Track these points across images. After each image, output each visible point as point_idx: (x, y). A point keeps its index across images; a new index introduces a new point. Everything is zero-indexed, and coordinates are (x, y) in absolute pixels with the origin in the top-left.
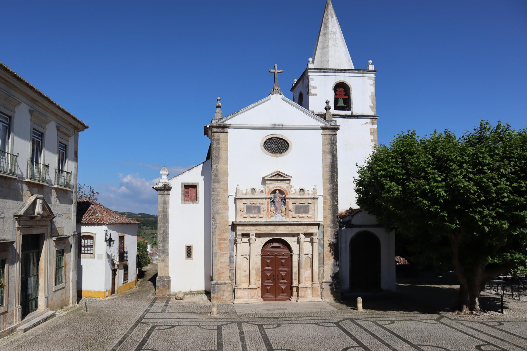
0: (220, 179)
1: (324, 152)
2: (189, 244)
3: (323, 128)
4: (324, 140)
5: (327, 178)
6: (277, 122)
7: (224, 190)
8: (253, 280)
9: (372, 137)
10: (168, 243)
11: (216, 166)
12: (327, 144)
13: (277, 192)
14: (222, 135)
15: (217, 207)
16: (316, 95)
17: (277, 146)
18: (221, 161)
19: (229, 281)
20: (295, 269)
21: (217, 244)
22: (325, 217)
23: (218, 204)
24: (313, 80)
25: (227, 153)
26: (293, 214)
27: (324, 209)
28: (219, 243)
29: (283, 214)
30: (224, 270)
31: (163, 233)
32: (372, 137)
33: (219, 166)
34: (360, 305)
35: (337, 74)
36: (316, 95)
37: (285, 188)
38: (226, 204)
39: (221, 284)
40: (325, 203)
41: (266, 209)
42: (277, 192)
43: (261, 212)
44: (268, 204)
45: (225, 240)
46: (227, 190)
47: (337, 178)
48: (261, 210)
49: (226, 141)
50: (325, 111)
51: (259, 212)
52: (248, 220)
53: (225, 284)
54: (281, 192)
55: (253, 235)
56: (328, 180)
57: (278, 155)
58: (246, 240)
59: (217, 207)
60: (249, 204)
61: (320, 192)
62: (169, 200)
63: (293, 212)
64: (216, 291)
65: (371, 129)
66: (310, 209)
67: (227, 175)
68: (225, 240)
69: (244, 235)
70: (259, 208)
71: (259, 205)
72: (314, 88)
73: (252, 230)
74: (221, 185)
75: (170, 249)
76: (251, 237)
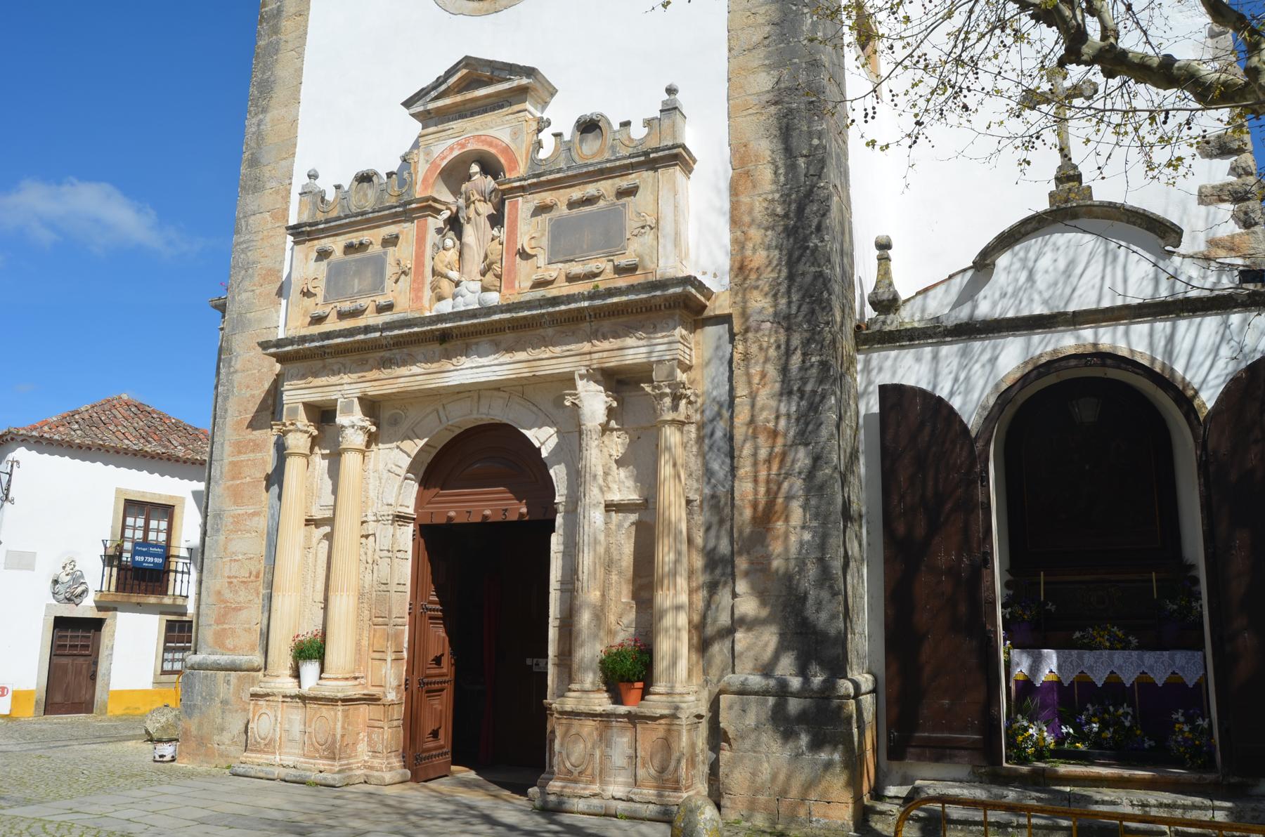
0: (267, 172)
5: (757, 37)
7: (274, 217)
11: (259, 125)
18: (280, 94)
21: (226, 469)
23: (246, 283)
25: (301, 56)
28: (233, 464)
30: (243, 596)
33: (268, 117)
42: (475, 168)
43: (389, 283)
48: (391, 269)
51: (378, 286)
53: (233, 668)
54: (490, 167)
55: (348, 410)
56: (761, 52)
59: (244, 296)
63: (542, 260)
64: (198, 700)
66: (632, 223)
76: (341, 419)
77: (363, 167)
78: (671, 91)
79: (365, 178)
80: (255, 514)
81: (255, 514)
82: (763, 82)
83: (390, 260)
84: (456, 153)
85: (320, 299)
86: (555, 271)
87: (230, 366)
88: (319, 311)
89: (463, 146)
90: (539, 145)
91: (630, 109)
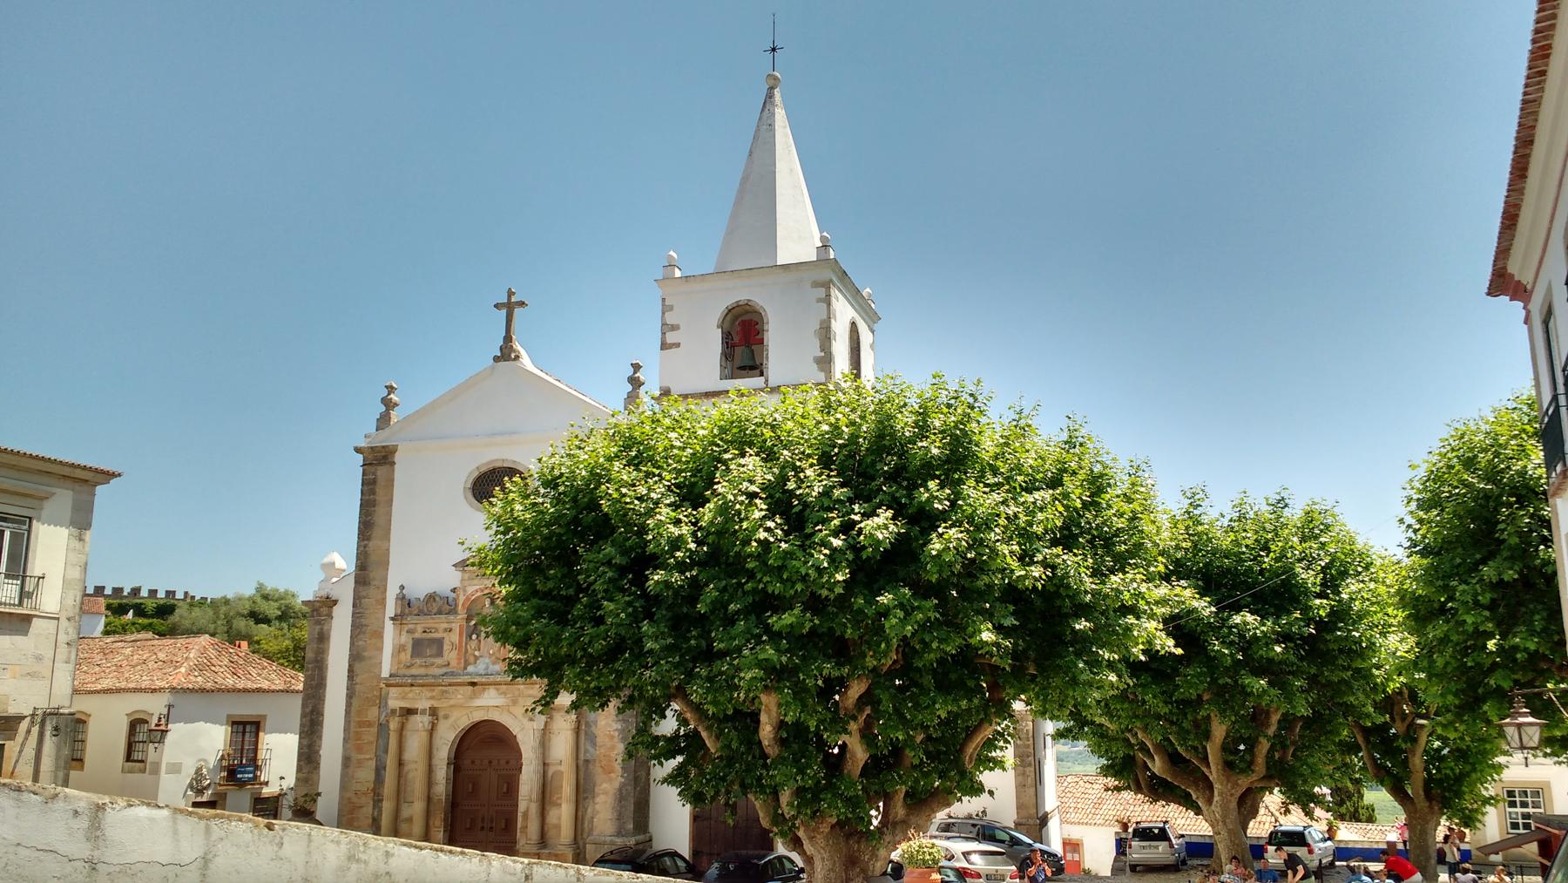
10: (320, 737)
14: (381, 472)
16: (678, 345)
18: (377, 532)
20: (522, 806)
24: (671, 308)
30: (364, 800)
31: (312, 712)
36: (678, 345)
43: (446, 653)
45: (370, 724)
46: (383, 602)
48: (446, 647)
49: (390, 482)
51: (440, 654)
55: (423, 712)
60: (417, 635)
67: (385, 563)
68: (370, 724)
70: (439, 643)
72: (674, 328)
74: (372, 591)
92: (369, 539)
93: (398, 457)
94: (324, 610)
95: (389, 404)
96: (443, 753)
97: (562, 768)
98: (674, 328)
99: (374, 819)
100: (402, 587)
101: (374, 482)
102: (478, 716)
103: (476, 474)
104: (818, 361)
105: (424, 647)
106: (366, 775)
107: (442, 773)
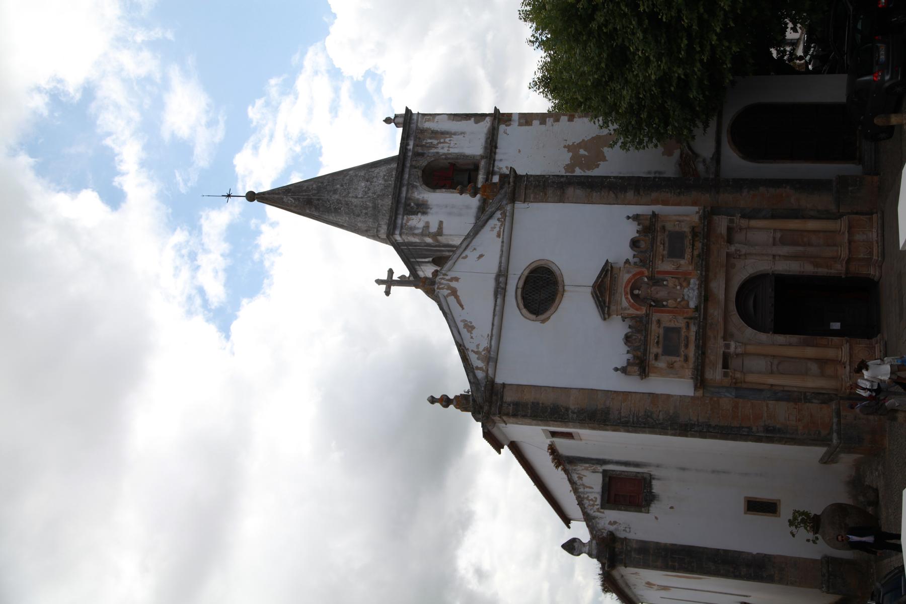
1: (561, 200)
2: (742, 506)
3: (513, 200)
4: (536, 200)
6: (491, 284)
8: (830, 353)
9: (536, 123)
10: (740, 553)
11: (573, 412)
12: (546, 194)
13: (636, 292)
14: (509, 397)
15: (661, 417)
16: (441, 223)
17: (540, 291)
19: (833, 406)
20: (808, 269)
22: (694, 204)
26: (685, 264)
27: (679, 204)
29: (684, 284)
32: (536, 123)
33: (572, 407)
34: (894, 120)
35: (405, 182)
36: (441, 223)
37: (630, 275)
38: (653, 397)
39: (839, 423)
40: (665, 203)
41: (670, 316)
43: (678, 325)
44: (663, 312)
47: (614, 177)
48: (672, 325)
50: (478, 196)
51: (677, 330)
52: (692, 351)
53: (838, 414)
55: (727, 346)
57: (560, 288)
58: (734, 363)
59: (661, 417)
60: (660, 351)
61: (644, 210)
62: (638, 541)
63: (682, 262)
65: (520, 125)
66: (677, 229)
67: (592, 393)
69: (725, 366)
70: (668, 330)
71: (661, 331)
73: (716, 347)
75: (755, 553)
77: (622, 343)
78: (628, 218)
79: (627, 339)
80: (767, 406)
81: (767, 406)
82: (630, 195)
83: (668, 325)
84: (629, 296)
85: (678, 359)
86: (688, 256)
87: (694, 425)
88: (682, 359)
89: (626, 294)
90: (635, 263)
91: (631, 230)
92: (567, 409)
93: (499, 380)
94: (618, 546)
95: (445, 401)
96: (763, 337)
97: (778, 235)
98: (427, 226)
99: (823, 402)
100: (616, 369)
101: (516, 405)
102: (733, 307)
103: (524, 311)
104: (476, 122)
105: (671, 344)
106: (783, 413)
107: (780, 338)
